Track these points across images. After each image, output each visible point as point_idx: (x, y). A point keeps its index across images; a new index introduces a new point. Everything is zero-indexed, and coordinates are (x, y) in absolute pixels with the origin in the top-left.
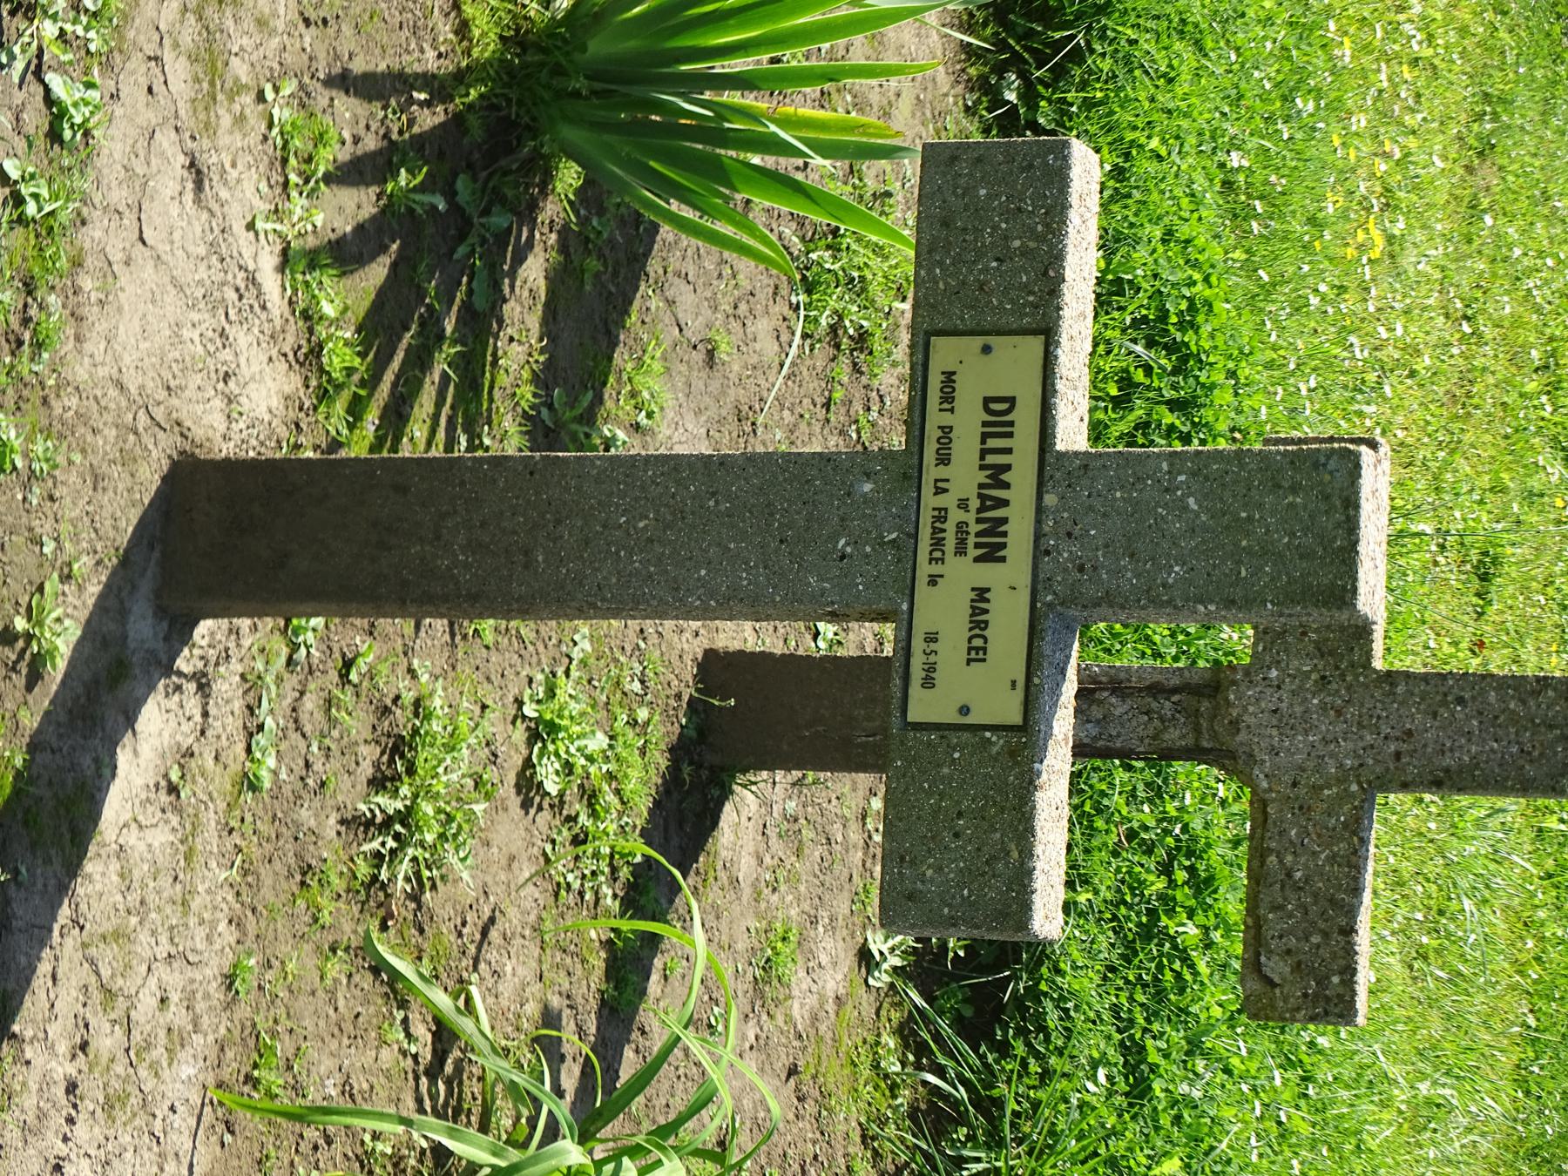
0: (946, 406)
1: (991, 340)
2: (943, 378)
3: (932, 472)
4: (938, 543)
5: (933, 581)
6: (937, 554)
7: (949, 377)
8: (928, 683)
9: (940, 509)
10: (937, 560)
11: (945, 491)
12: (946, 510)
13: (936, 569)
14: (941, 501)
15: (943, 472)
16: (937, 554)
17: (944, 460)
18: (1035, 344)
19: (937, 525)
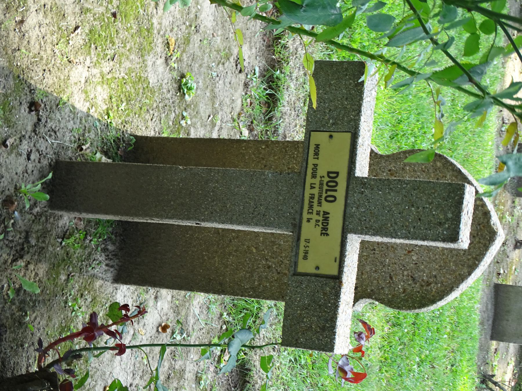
0: (316, 157)
1: (332, 133)
2: (315, 146)
3: (309, 180)
4: (311, 207)
6: (310, 211)
7: (317, 146)
9: (312, 194)
10: (310, 213)
11: (314, 188)
12: (314, 195)
13: (310, 216)
15: (313, 181)
16: (310, 211)
17: (314, 176)
19: (311, 200)
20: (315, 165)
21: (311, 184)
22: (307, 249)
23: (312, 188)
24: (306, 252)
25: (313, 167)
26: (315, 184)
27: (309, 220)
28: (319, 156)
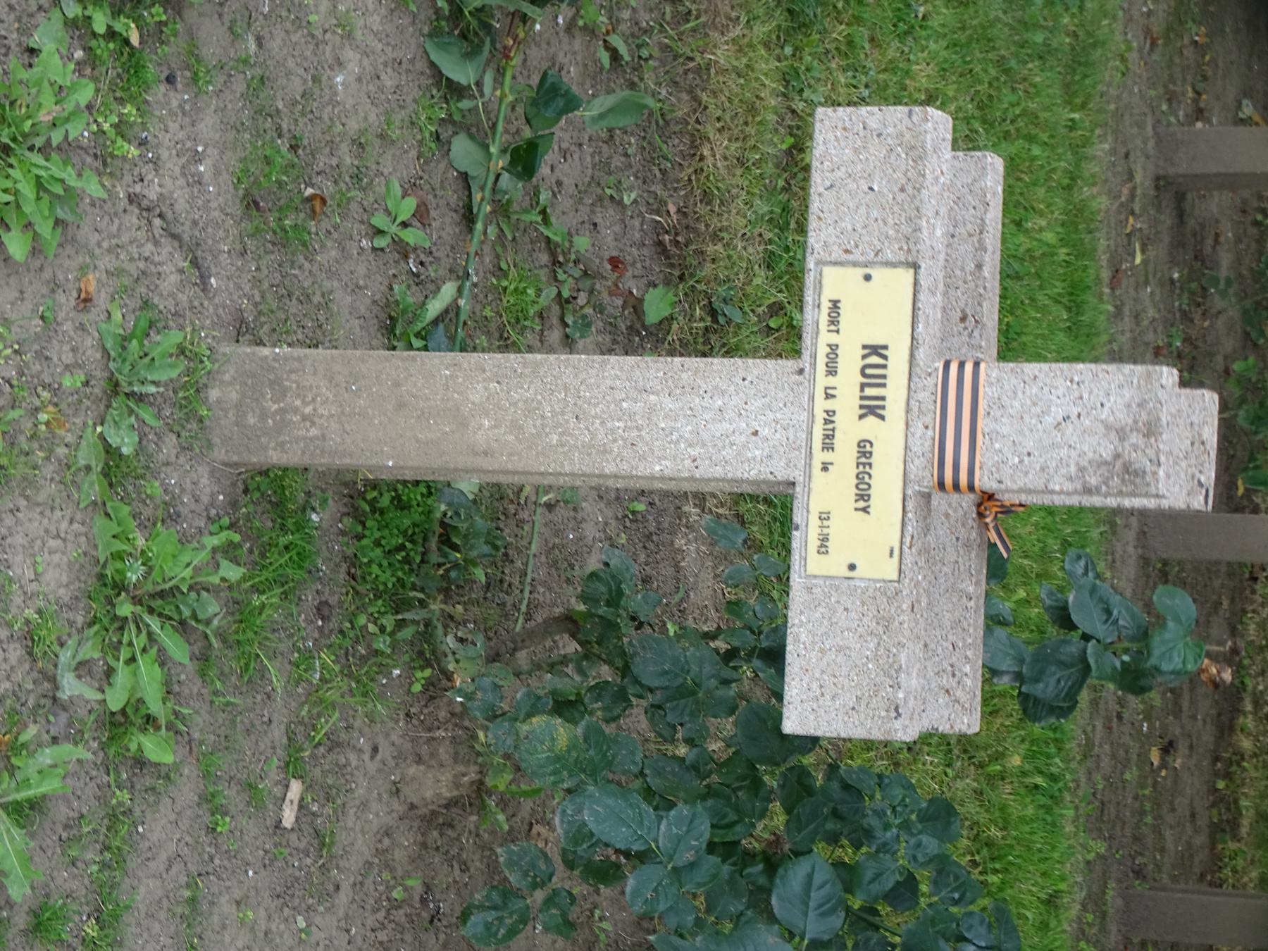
2: (830, 305)
3: (822, 380)
4: (829, 437)
5: (825, 469)
7: (835, 304)
8: (823, 548)
11: (833, 396)
14: (830, 404)
15: (831, 381)
17: (832, 372)
18: (906, 276)
20: (833, 348)
21: (826, 388)
22: (825, 531)
23: (828, 396)
24: (824, 539)
25: (828, 350)
26: (834, 388)
27: (825, 468)
28: (841, 326)
